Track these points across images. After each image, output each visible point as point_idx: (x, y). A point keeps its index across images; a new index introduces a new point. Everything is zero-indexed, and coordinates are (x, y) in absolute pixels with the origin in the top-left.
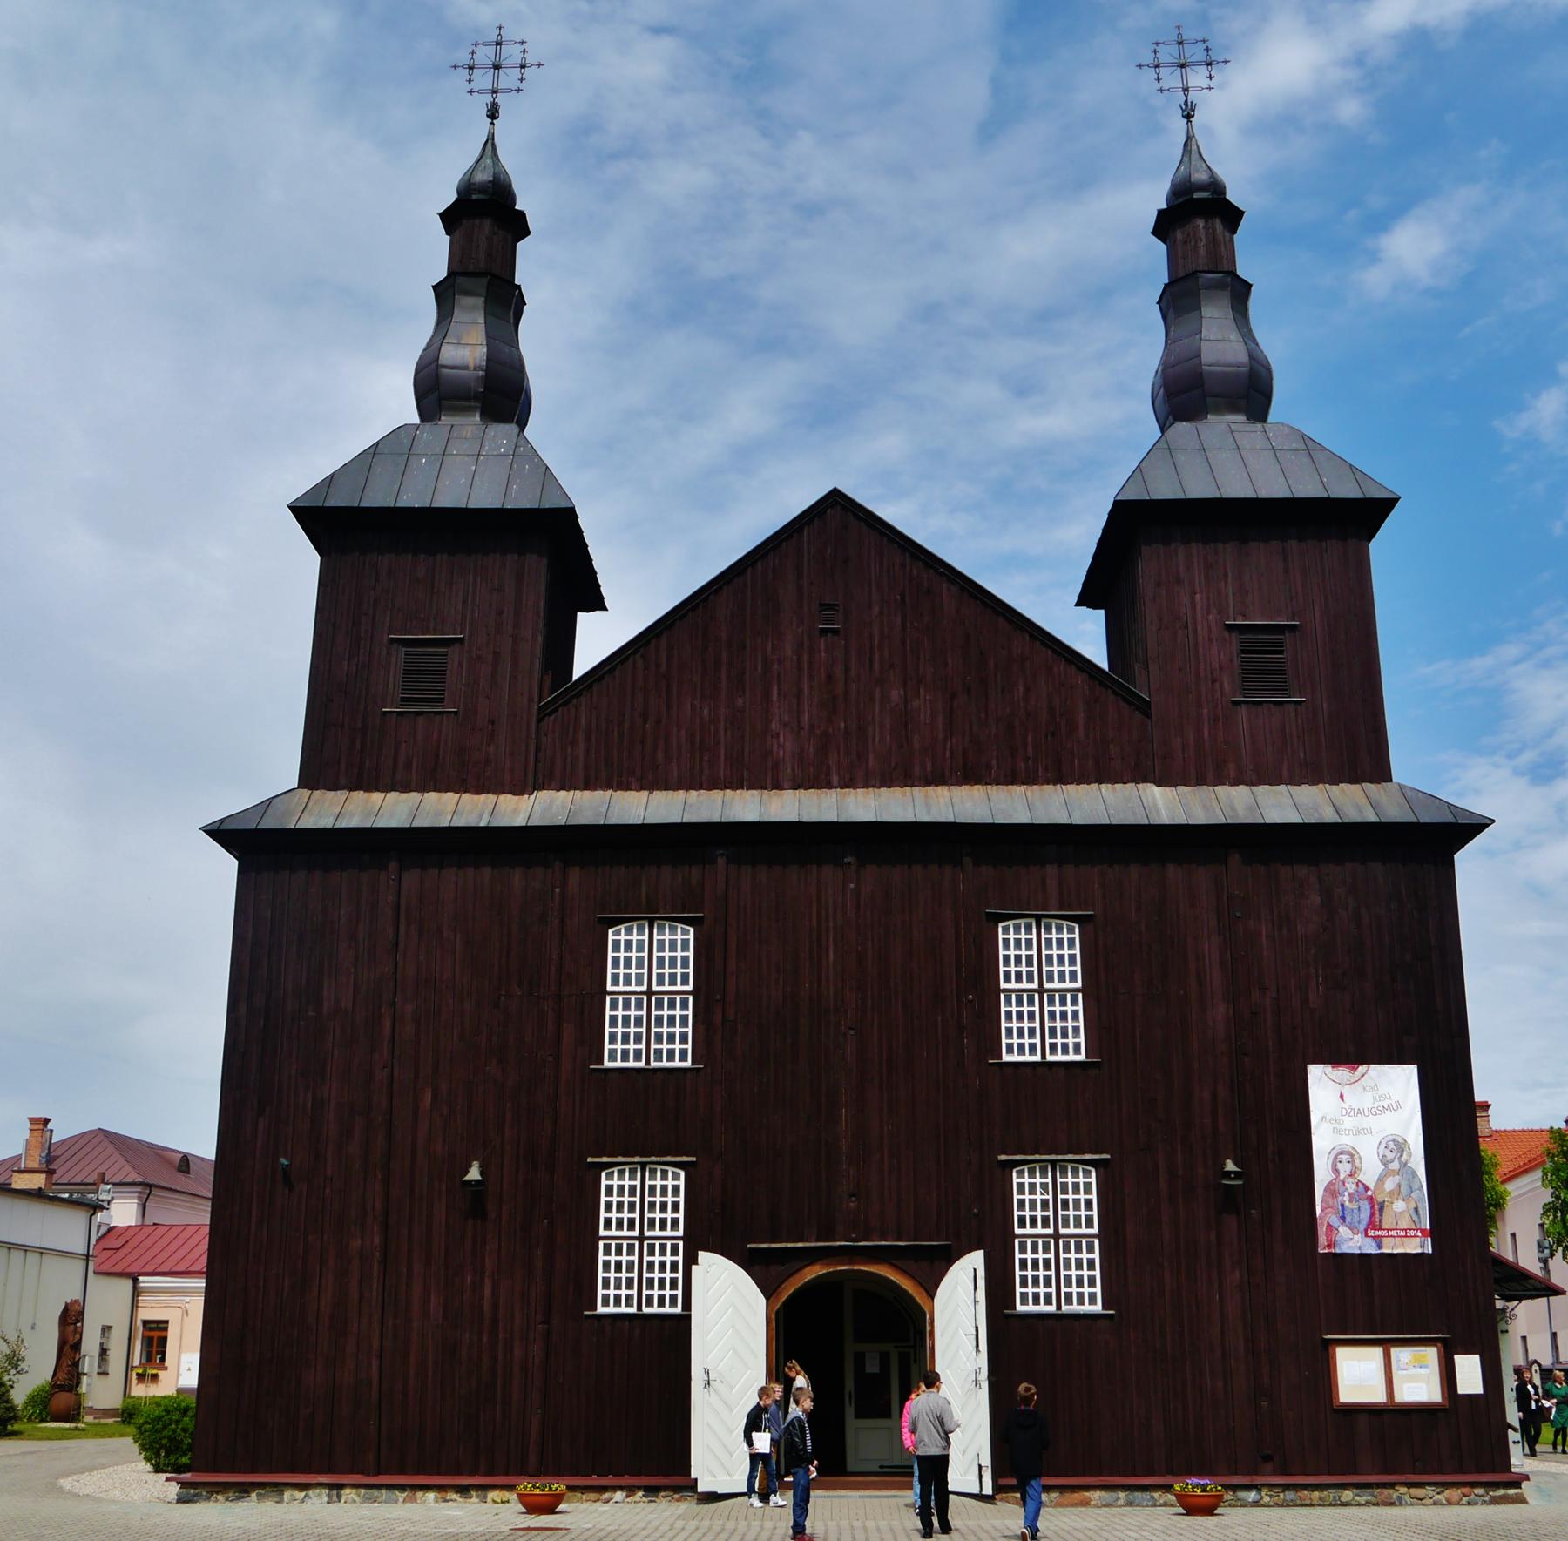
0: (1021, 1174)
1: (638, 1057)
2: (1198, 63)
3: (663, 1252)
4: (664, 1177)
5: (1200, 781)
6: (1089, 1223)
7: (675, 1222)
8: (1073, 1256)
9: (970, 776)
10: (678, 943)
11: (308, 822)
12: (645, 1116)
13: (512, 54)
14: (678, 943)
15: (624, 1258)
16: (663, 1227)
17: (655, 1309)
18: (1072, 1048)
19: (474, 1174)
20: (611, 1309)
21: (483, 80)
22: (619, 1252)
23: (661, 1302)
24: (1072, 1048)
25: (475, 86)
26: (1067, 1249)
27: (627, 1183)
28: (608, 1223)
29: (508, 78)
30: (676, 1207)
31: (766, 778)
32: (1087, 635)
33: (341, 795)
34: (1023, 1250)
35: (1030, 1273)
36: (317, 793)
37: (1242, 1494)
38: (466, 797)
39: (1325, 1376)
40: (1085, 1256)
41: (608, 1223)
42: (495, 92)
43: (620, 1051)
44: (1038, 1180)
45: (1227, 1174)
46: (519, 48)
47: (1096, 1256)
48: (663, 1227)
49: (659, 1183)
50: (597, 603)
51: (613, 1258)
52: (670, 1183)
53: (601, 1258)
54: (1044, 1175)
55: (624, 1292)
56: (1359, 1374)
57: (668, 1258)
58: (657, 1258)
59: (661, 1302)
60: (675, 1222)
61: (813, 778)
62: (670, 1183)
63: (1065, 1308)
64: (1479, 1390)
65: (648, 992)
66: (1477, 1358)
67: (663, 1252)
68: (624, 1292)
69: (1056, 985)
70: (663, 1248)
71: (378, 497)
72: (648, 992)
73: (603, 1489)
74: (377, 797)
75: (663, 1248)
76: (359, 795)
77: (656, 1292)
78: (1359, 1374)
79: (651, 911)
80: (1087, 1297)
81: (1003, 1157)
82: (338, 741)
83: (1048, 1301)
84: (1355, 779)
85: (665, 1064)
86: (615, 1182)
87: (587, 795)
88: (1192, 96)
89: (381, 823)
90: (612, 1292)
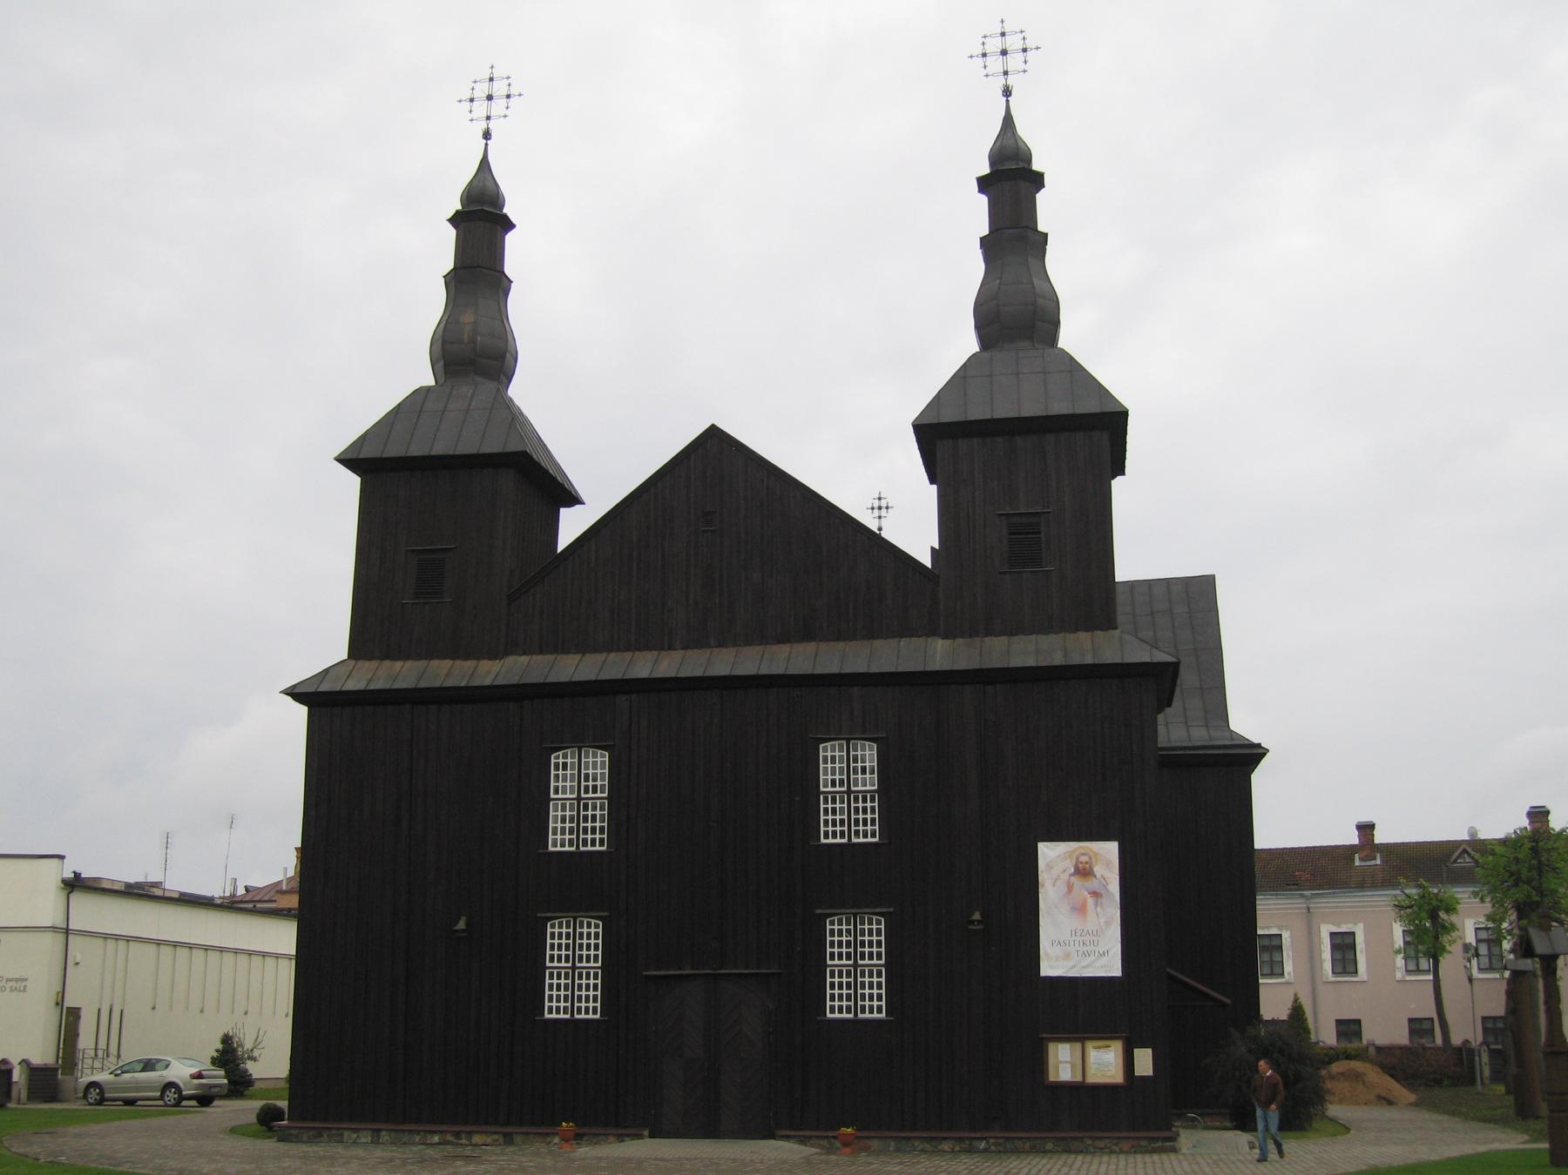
0: (832, 923)
1: (571, 844)
2: (1016, 51)
3: (588, 978)
4: (589, 926)
5: (972, 633)
6: (879, 957)
7: (596, 956)
8: (867, 980)
9: (807, 633)
10: (598, 763)
11: (351, 686)
12: (576, 884)
13: (499, 88)
14: (598, 763)
15: (563, 981)
16: (871, 957)
17: (583, 1016)
18: (868, 835)
19: (461, 925)
20: (554, 1016)
21: (480, 108)
22: (559, 977)
23: (587, 1012)
24: (868, 835)
25: (474, 115)
26: (863, 975)
27: (564, 930)
28: (552, 957)
29: (498, 107)
30: (879, 943)
31: (662, 642)
32: (912, 521)
33: (375, 663)
34: (832, 976)
35: (875, 991)
36: (360, 663)
37: (976, 1143)
38: (458, 662)
39: (1039, 1062)
40: (875, 980)
41: (552, 957)
42: (488, 118)
43: (559, 840)
44: (844, 927)
45: (972, 922)
46: (506, 82)
47: (883, 980)
48: (559, 960)
49: (585, 930)
50: (573, 499)
51: (555, 981)
52: (593, 930)
53: (548, 981)
54: (848, 924)
55: (562, 1004)
56: (1063, 1062)
57: (592, 982)
58: (584, 982)
59: (587, 1012)
60: (596, 956)
61: (697, 640)
62: (593, 930)
63: (860, 1016)
64: (1150, 1073)
65: (577, 796)
66: (1149, 1051)
67: (588, 978)
68: (562, 1004)
69: (860, 788)
70: (588, 975)
71: (394, 451)
72: (577, 796)
73: (547, 1134)
74: (398, 664)
75: (588, 975)
76: (387, 663)
77: (583, 1005)
78: (1063, 1062)
79: (581, 740)
80: (875, 1009)
81: (818, 911)
82: (372, 626)
83: (849, 1011)
84: (1087, 630)
85: (589, 848)
86: (557, 930)
87: (540, 657)
88: (1011, 80)
89: (396, 686)
90: (554, 1004)
